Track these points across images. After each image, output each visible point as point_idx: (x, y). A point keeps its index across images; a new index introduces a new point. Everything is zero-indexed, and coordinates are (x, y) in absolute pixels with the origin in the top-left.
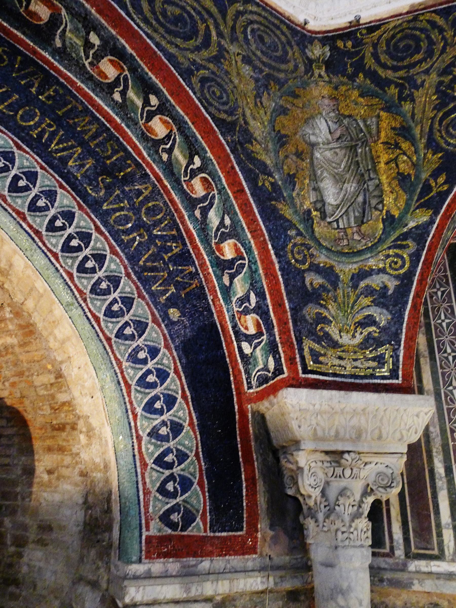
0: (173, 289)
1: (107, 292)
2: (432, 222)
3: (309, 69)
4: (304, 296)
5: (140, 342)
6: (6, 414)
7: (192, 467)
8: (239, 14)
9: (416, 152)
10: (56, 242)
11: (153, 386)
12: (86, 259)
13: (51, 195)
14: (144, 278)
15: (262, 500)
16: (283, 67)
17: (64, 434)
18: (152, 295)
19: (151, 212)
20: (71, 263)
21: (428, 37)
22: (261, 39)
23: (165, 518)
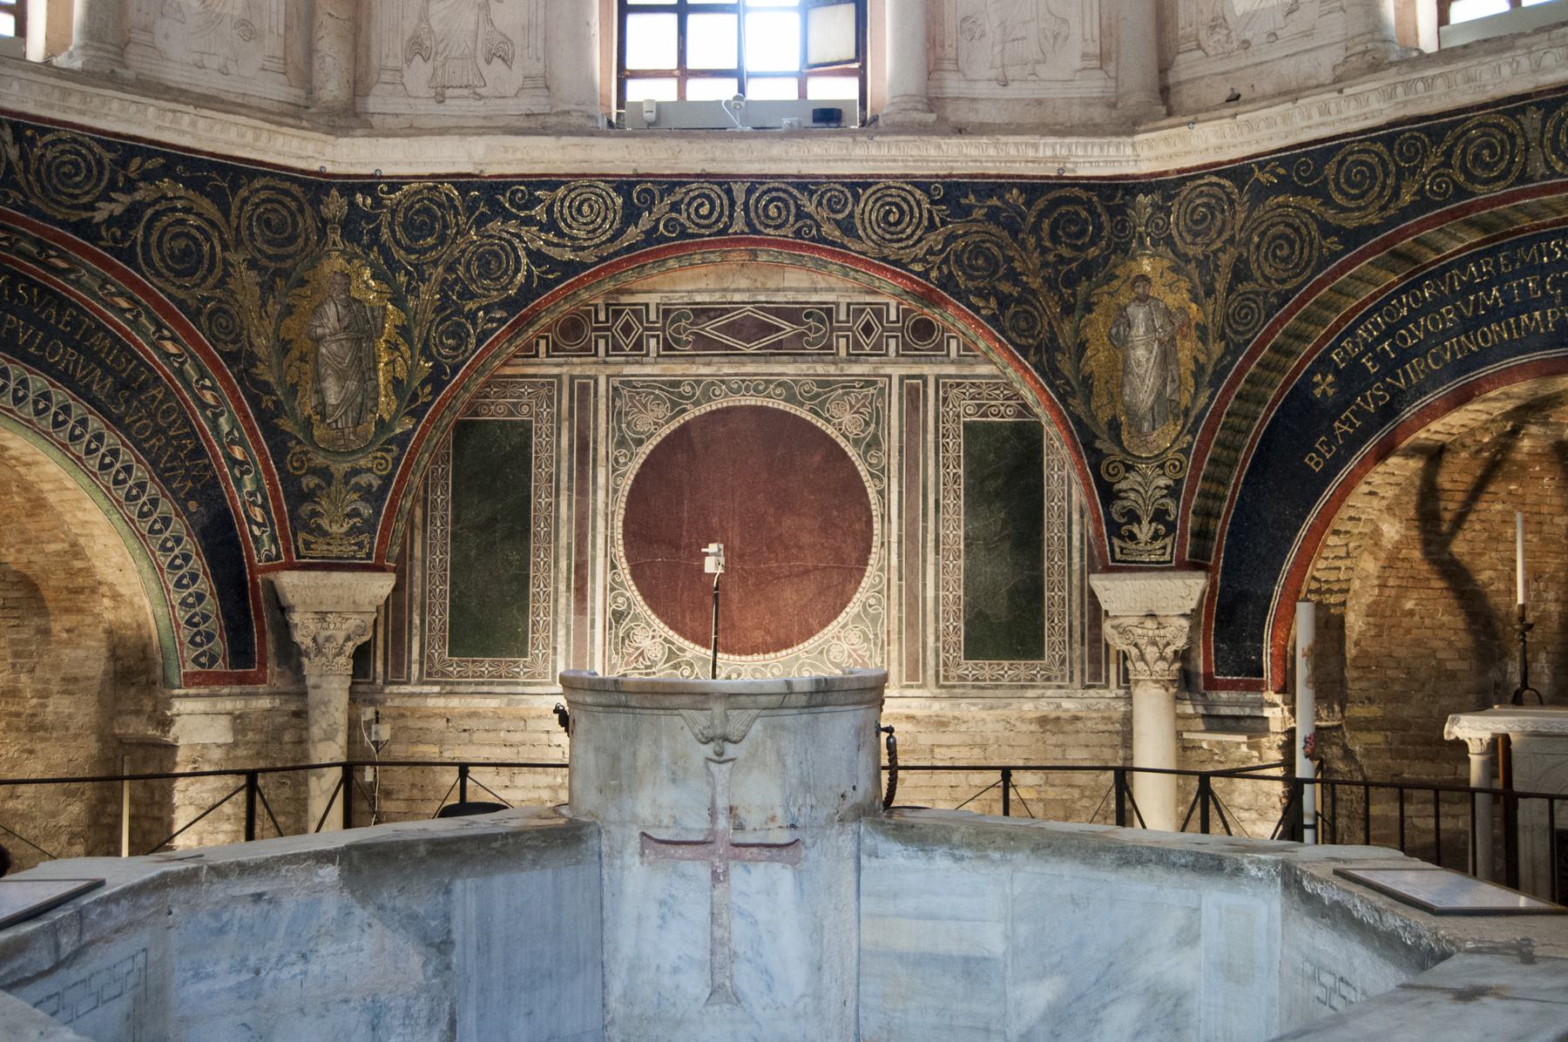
0: (190, 484)
1: (137, 497)
2: (414, 430)
3: (322, 234)
4: (299, 497)
5: (167, 534)
6: (10, 578)
7: (214, 624)
8: (245, 201)
9: (412, 357)
10: (93, 464)
11: (180, 567)
12: (118, 472)
13: (83, 422)
14: (165, 478)
15: (270, 647)
16: (291, 249)
17: (82, 597)
18: (173, 492)
19: (167, 413)
20: (108, 479)
21: (443, 217)
22: (268, 222)
23: (196, 660)
